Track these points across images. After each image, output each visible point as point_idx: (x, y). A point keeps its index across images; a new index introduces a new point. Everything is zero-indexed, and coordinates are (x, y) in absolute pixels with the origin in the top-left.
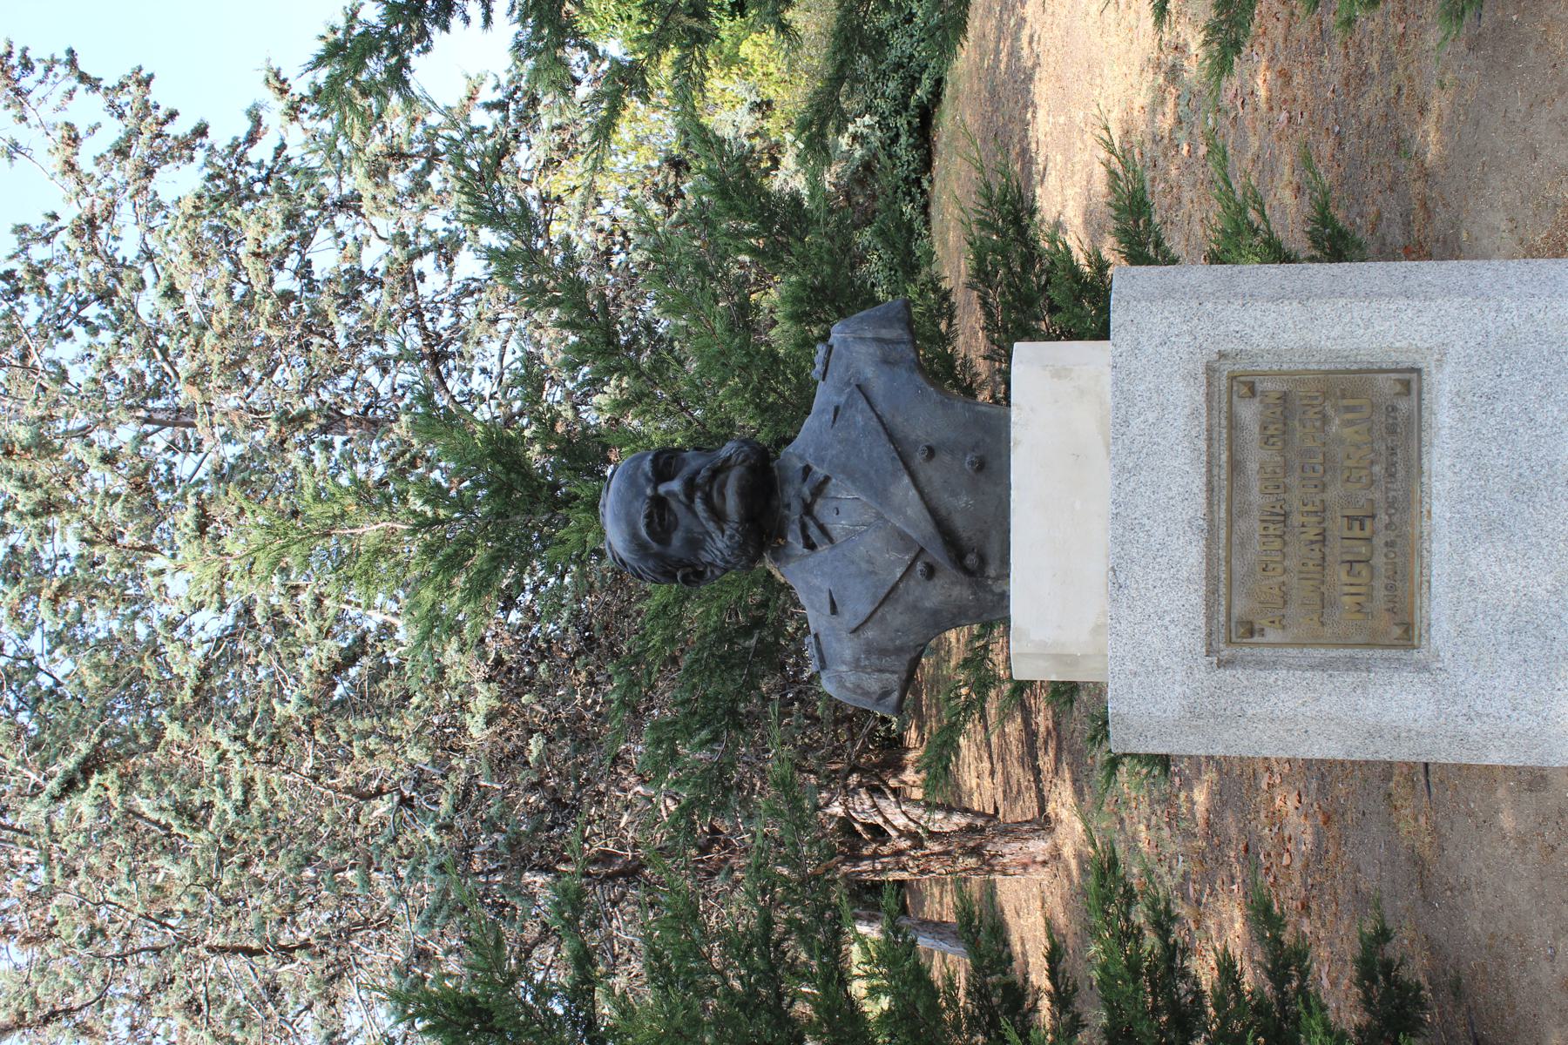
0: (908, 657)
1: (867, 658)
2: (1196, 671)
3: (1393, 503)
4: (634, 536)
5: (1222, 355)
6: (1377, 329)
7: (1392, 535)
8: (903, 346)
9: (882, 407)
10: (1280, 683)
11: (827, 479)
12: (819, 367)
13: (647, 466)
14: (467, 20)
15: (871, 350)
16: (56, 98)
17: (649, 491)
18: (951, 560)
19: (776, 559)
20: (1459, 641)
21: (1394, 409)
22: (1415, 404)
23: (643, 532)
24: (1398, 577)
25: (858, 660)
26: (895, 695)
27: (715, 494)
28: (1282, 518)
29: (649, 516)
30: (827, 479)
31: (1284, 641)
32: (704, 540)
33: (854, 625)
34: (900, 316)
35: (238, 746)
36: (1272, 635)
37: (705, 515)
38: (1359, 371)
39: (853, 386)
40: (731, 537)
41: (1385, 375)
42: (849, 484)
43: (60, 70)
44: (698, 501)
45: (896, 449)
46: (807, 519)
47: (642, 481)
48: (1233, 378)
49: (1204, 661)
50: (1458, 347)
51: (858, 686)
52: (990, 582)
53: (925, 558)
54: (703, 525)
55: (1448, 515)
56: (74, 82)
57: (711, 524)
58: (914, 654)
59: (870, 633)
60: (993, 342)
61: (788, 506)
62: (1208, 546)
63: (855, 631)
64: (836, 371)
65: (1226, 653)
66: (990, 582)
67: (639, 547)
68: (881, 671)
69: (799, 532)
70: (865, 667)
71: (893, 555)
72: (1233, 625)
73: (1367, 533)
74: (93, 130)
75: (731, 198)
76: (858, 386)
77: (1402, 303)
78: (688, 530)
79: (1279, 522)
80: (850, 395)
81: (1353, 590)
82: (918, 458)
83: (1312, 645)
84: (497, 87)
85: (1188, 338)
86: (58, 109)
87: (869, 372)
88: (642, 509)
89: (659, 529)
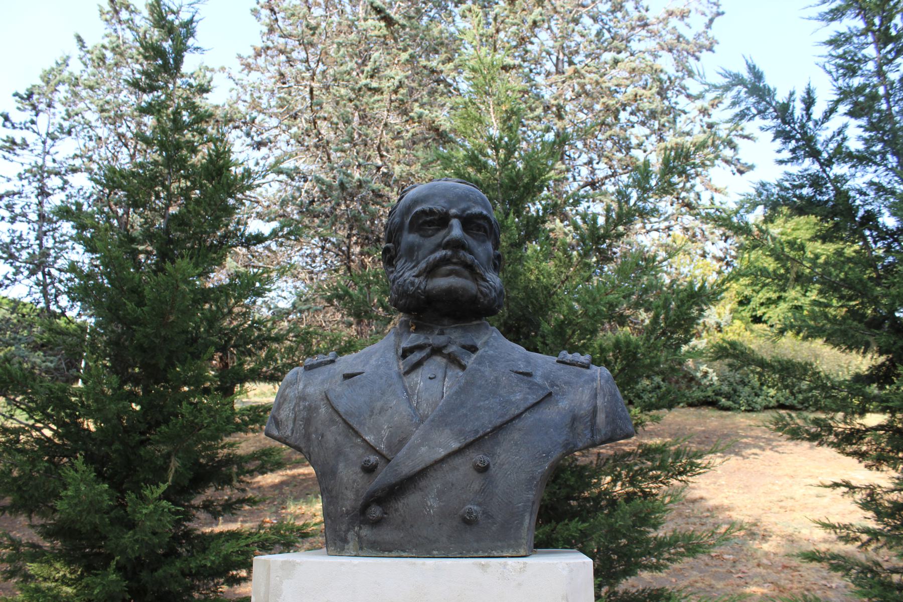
0: (302, 445)
1: (305, 407)
8: (589, 436)
9: (529, 419)
11: (463, 367)
12: (569, 357)
13: (476, 210)
14: (779, 151)
15: (585, 405)
16: (701, 8)
17: (453, 211)
18: (374, 492)
23: (418, 208)
26: (275, 433)
27: (449, 267)
29: (431, 212)
30: (463, 367)
32: (412, 261)
33: (331, 396)
34: (618, 431)
35: (397, 83)
37: (431, 260)
39: (550, 389)
40: (412, 283)
42: (455, 388)
43: (715, 9)
45: (487, 434)
46: (428, 350)
47: (463, 206)
51: (285, 400)
52: (356, 529)
53: (382, 462)
56: (710, 17)
59: (323, 410)
60: (608, 459)
61: (442, 333)
64: (565, 372)
66: (356, 529)
71: (385, 433)
74: (688, 25)
75: (688, 301)
76: (550, 394)
78: (420, 247)
80: (542, 387)
82: (477, 457)
84: (722, 204)
86: (696, 10)
87: (564, 404)
88: (438, 205)
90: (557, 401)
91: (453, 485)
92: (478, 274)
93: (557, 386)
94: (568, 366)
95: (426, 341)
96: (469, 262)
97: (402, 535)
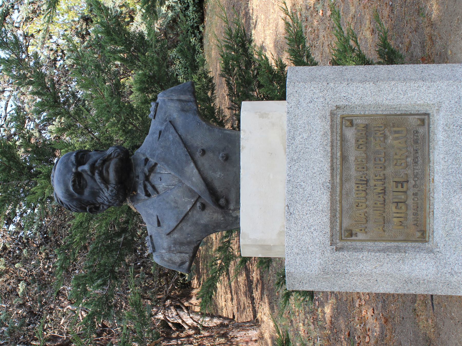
0: (193, 246)
1: (174, 247)
2: (326, 253)
3: (417, 175)
4: (67, 190)
5: (338, 107)
6: (409, 95)
7: (416, 190)
8: (191, 103)
9: (181, 131)
10: (364, 258)
11: (156, 164)
12: (152, 113)
13: (73, 158)
15: (176, 105)
17: (74, 170)
18: (213, 201)
19: (132, 201)
20: (447, 239)
21: (417, 132)
22: (427, 130)
23: (71, 189)
24: (419, 209)
25: (170, 247)
26: (187, 264)
27: (104, 172)
28: (365, 182)
29: (74, 181)
30: (156, 164)
31: (366, 239)
32: (99, 192)
33: (168, 231)
34: (189, 89)
36: (361, 236)
37: (100, 181)
38: (401, 115)
39: (168, 121)
40: (112, 191)
41: (413, 117)
42: (166, 167)
44: (96, 174)
46: (147, 183)
47: (71, 165)
48: (343, 118)
49: (329, 248)
50: (446, 104)
51: (170, 260)
52: (231, 212)
53: (200, 200)
54: (98, 185)
55: (442, 181)
57: (103, 185)
58: (196, 245)
59: (175, 235)
60: (232, 101)
61: (138, 177)
62: (331, 195)
63: (169, 234)
64: (160, 115)
65: (340, 244)
66: (231, 212)
67: (70, 196)
68: (181, 253)
69: (143, 189)
70: (173, 251)
71: (186, 200)
72: (343, 231)
73: (404, 189)
75: (112, 35)
76: (170, 122)
77: (421, 83)
78: (92, 188)
79: (364, 184)
80: (167, 126)
81: (398, 215)
82: (198, 154)
83: (379, 240)
85: (322, 100)
87: (175, 115)
88: (70, 178)
89: (78, 187)
90: (174, 118)
91: (210, 166)
92: (107, 158)
93: (166, 118)
94: (157, 113)
95: (142, 184)
96: (102, 161)
97: (233, 189)
